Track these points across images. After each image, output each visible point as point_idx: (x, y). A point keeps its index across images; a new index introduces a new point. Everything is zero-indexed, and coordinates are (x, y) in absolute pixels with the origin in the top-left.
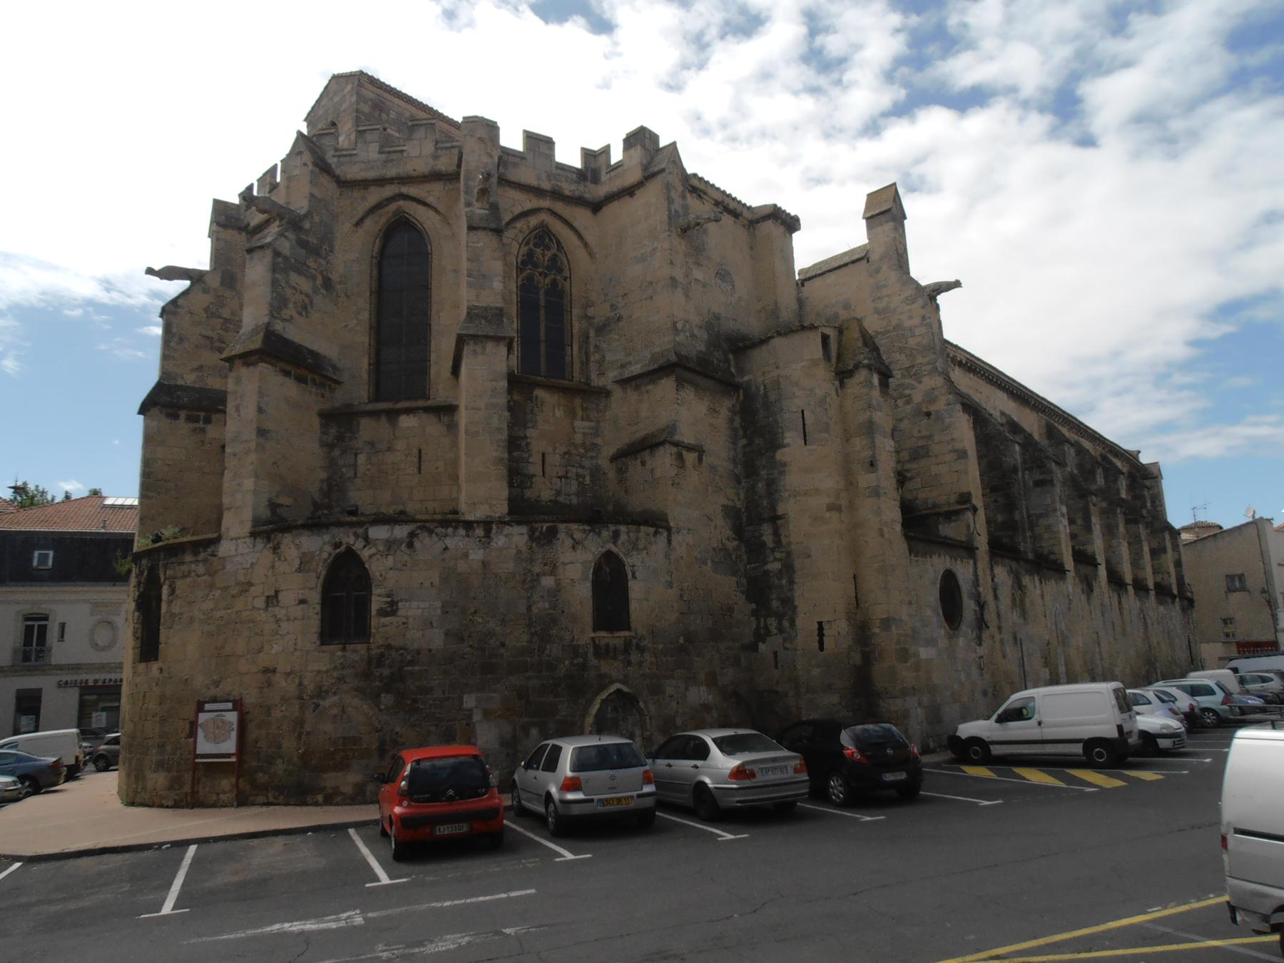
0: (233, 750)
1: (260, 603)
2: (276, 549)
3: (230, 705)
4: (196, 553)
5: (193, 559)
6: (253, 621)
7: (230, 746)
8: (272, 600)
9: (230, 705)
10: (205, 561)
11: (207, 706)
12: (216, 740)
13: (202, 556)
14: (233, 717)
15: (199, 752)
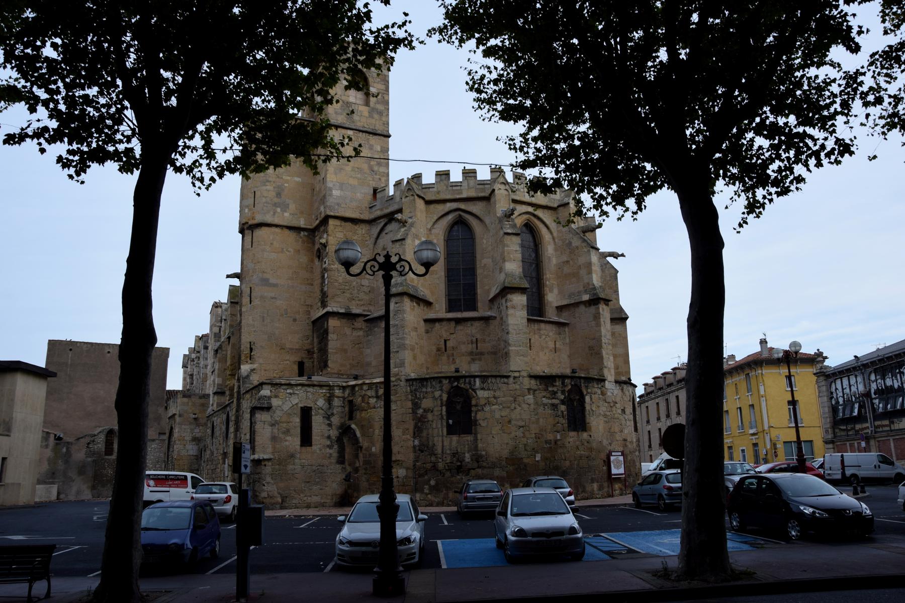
0: (623, 472)
1: (620, 411)
2: (622, 390)
3: (620, 454)
4: (598, 384)
5: (596, 386)
6: (618, 419)
7: (622, 471)
8: (623, 411)
9: (620, 454)
10: (600, 388)
11: (613, 454)
12: (618, 468)
13: (600, 386)
14: (621, 458)
15: (613, 473)
